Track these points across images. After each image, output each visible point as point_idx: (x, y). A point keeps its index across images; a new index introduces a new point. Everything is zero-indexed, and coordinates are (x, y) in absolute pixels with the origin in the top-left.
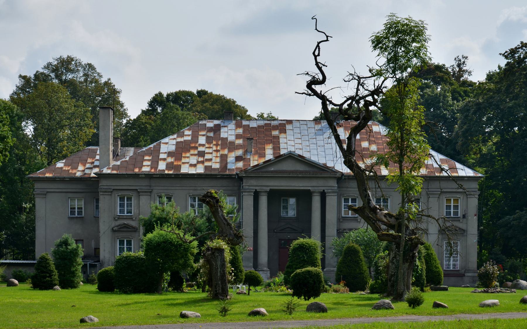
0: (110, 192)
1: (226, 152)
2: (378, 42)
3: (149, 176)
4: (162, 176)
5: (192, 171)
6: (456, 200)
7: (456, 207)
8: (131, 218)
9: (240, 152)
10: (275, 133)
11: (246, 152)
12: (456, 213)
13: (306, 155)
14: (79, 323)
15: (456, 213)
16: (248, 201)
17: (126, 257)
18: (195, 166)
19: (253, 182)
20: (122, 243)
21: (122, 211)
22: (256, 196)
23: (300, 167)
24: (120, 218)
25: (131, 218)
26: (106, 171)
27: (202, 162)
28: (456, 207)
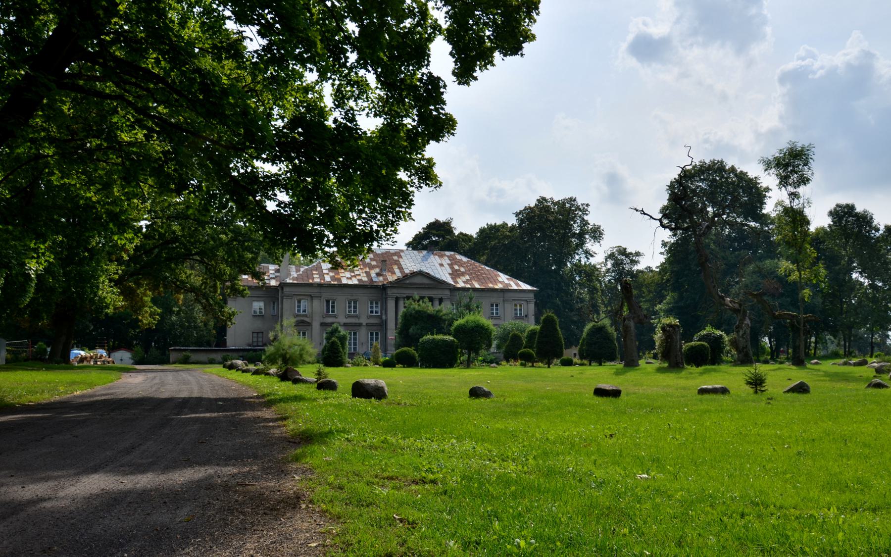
0: (290, 296)
1: (368, 270)
2: (831, 214)
3: (320, 285)
4: (329, 286)
5: (350, 282)
6: (520, 306)
7: (520, 310)
8: (306, 316)
9: (377, 270)
10: (395, 258)
11: (381, 270)
12: (521, 314)
13: (432, 273)
14: (465, 399)
15: (521, 314)
16: (391, 304)
17: (688, 350)
18: (350, 278)
19: (395, 291)
20: (372, 334)
21: (299, 311)
22: (397, 300)
23: (426, 281)
24: (297, 316)
25: (306, 316)
26: (288, 281)
27: (355, 276)
28: (520, 310)
